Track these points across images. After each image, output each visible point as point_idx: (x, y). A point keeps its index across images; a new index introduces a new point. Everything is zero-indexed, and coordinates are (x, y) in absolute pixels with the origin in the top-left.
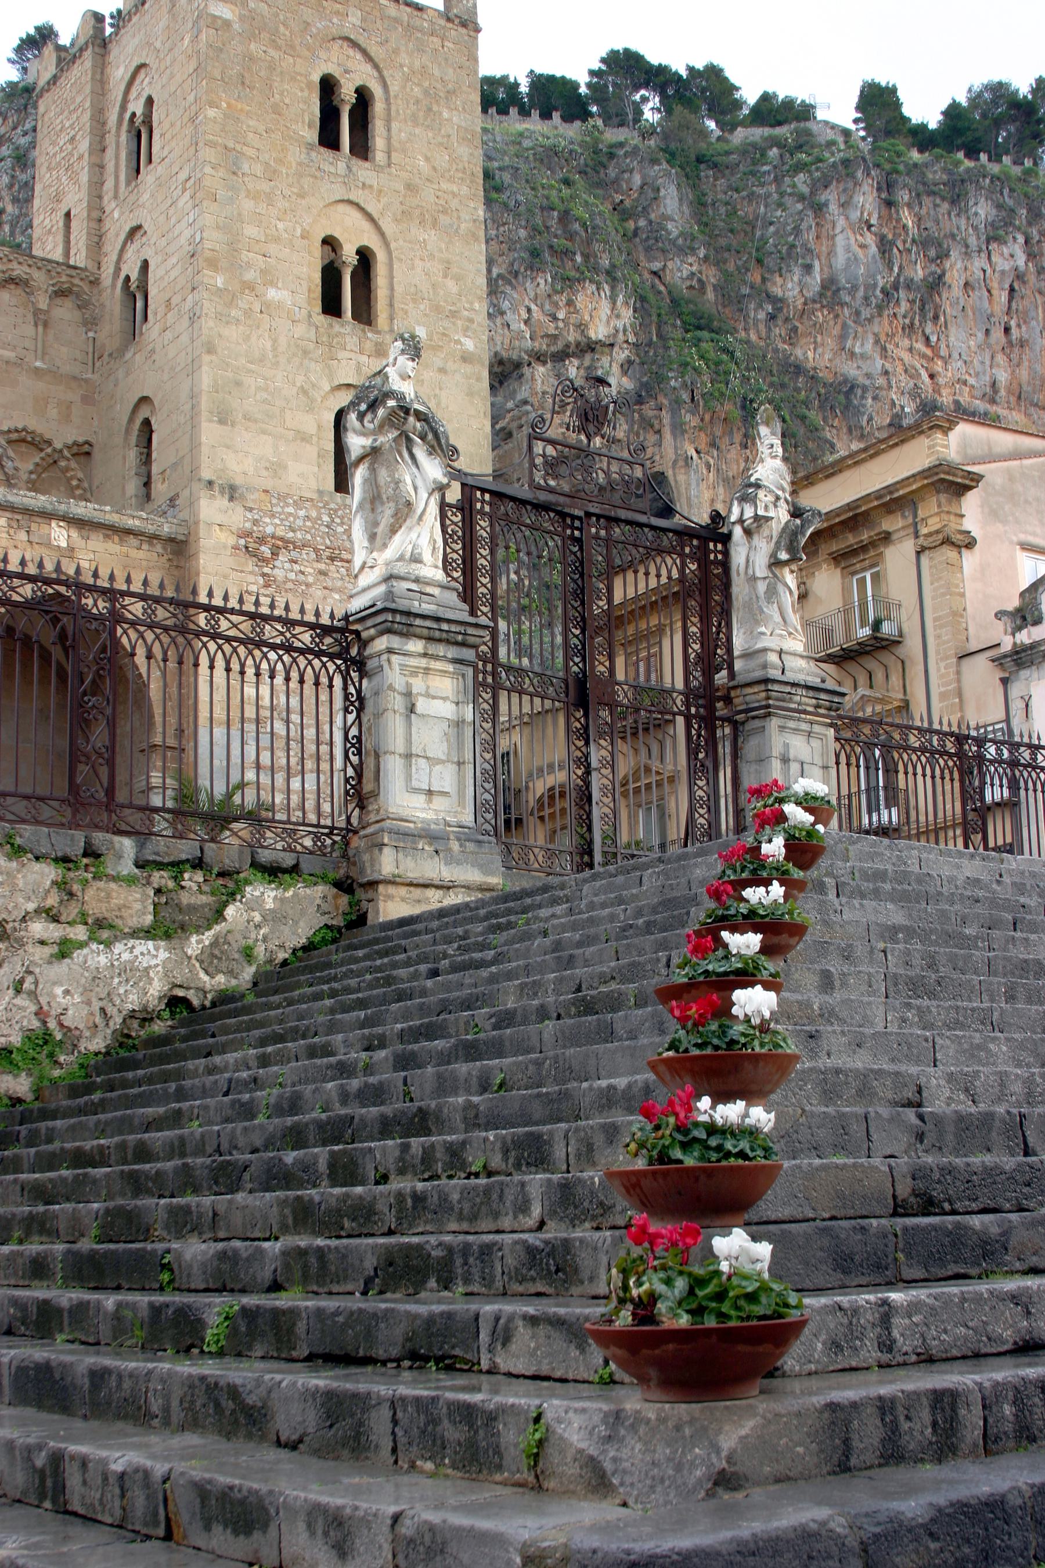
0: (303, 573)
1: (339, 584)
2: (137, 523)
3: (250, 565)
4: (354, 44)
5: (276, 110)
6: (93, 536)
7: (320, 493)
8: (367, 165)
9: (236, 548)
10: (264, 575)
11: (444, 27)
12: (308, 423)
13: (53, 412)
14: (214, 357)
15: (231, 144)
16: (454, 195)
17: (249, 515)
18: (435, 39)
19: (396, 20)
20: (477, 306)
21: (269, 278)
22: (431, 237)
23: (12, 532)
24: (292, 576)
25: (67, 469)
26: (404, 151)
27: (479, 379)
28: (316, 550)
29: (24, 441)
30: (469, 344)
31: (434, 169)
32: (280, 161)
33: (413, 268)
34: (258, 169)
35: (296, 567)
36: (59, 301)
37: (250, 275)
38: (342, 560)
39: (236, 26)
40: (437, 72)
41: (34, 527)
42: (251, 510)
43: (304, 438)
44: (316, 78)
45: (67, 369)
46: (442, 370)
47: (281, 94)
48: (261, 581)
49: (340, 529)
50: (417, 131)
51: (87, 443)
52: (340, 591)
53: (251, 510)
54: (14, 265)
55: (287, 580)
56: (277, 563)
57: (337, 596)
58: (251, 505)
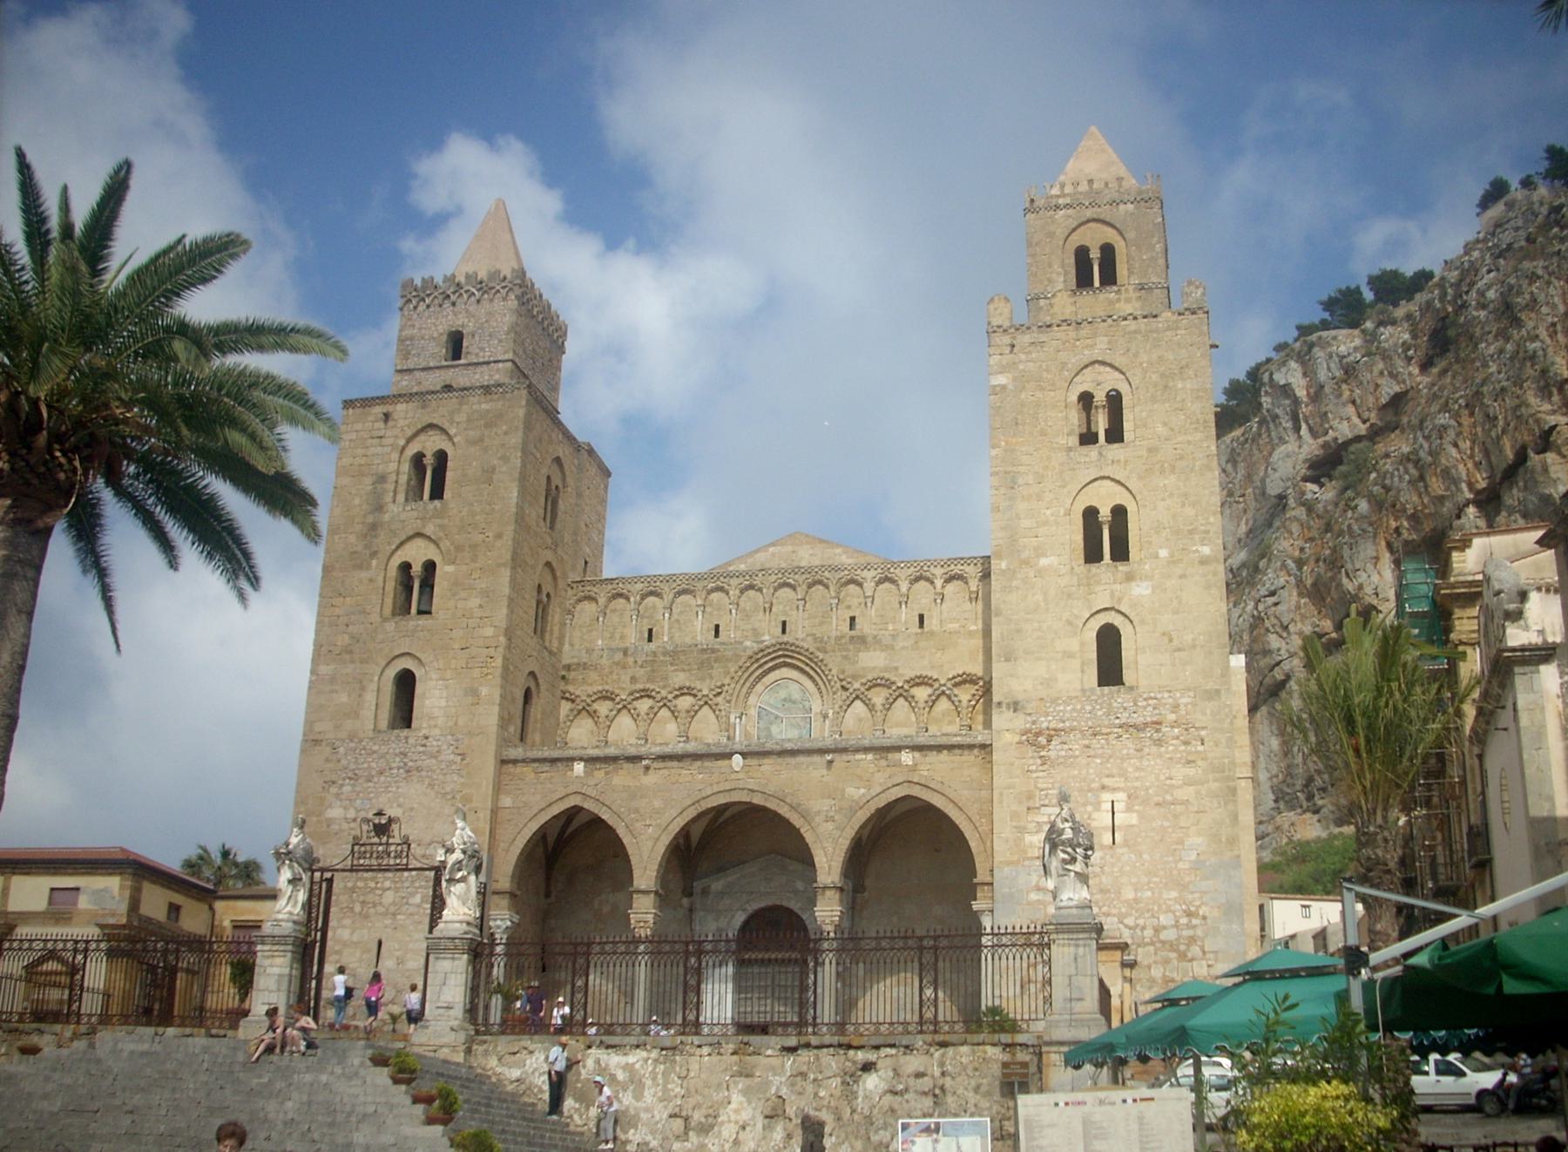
1: (1100, 751)
2: (959, 738)
3: (1030, 751)
4: (1103, 363)
5: (1043, 433)
6: (929, 753)
7: (1083, 691)
8: (1116, 446)
9: (1018, 743)
10: (1041, 757)
11: (1176, 321)
12: (1074, 644)
14: (1001, 618)
15: (1009, 469)
16: (1189, 443)
17: (1029, 719)
18: (1169, 333)
19: (1135, 332)
20: (1212, 519)
21: (1040, 552)
22: (1170, 481)
24: (1063, 753)
26: (1145, 425)
27: (1215, 574)
28: (1082, 732)
30: (1206, 550)
31: (1172, 429)
32: (1046, 468)
33: (1155, 508)
34: (1030, 479)
35: (1066, 747)
37: (1024, 555)
39: (1011, 387)
40: (1171, 357)
41: (890, 756)
42: (1030, 714)
43: (1069, 655)
44: (1074, 398)
46: (1182, 576)
47: (1046, 421)
48: (1039, 761)
49: (1100, 713)
50: (1156, 406)
52: (1101, 756)
53: (1030, 714)
55: (1059, 757)
57: (1098, 761)
58: (1029, 711)
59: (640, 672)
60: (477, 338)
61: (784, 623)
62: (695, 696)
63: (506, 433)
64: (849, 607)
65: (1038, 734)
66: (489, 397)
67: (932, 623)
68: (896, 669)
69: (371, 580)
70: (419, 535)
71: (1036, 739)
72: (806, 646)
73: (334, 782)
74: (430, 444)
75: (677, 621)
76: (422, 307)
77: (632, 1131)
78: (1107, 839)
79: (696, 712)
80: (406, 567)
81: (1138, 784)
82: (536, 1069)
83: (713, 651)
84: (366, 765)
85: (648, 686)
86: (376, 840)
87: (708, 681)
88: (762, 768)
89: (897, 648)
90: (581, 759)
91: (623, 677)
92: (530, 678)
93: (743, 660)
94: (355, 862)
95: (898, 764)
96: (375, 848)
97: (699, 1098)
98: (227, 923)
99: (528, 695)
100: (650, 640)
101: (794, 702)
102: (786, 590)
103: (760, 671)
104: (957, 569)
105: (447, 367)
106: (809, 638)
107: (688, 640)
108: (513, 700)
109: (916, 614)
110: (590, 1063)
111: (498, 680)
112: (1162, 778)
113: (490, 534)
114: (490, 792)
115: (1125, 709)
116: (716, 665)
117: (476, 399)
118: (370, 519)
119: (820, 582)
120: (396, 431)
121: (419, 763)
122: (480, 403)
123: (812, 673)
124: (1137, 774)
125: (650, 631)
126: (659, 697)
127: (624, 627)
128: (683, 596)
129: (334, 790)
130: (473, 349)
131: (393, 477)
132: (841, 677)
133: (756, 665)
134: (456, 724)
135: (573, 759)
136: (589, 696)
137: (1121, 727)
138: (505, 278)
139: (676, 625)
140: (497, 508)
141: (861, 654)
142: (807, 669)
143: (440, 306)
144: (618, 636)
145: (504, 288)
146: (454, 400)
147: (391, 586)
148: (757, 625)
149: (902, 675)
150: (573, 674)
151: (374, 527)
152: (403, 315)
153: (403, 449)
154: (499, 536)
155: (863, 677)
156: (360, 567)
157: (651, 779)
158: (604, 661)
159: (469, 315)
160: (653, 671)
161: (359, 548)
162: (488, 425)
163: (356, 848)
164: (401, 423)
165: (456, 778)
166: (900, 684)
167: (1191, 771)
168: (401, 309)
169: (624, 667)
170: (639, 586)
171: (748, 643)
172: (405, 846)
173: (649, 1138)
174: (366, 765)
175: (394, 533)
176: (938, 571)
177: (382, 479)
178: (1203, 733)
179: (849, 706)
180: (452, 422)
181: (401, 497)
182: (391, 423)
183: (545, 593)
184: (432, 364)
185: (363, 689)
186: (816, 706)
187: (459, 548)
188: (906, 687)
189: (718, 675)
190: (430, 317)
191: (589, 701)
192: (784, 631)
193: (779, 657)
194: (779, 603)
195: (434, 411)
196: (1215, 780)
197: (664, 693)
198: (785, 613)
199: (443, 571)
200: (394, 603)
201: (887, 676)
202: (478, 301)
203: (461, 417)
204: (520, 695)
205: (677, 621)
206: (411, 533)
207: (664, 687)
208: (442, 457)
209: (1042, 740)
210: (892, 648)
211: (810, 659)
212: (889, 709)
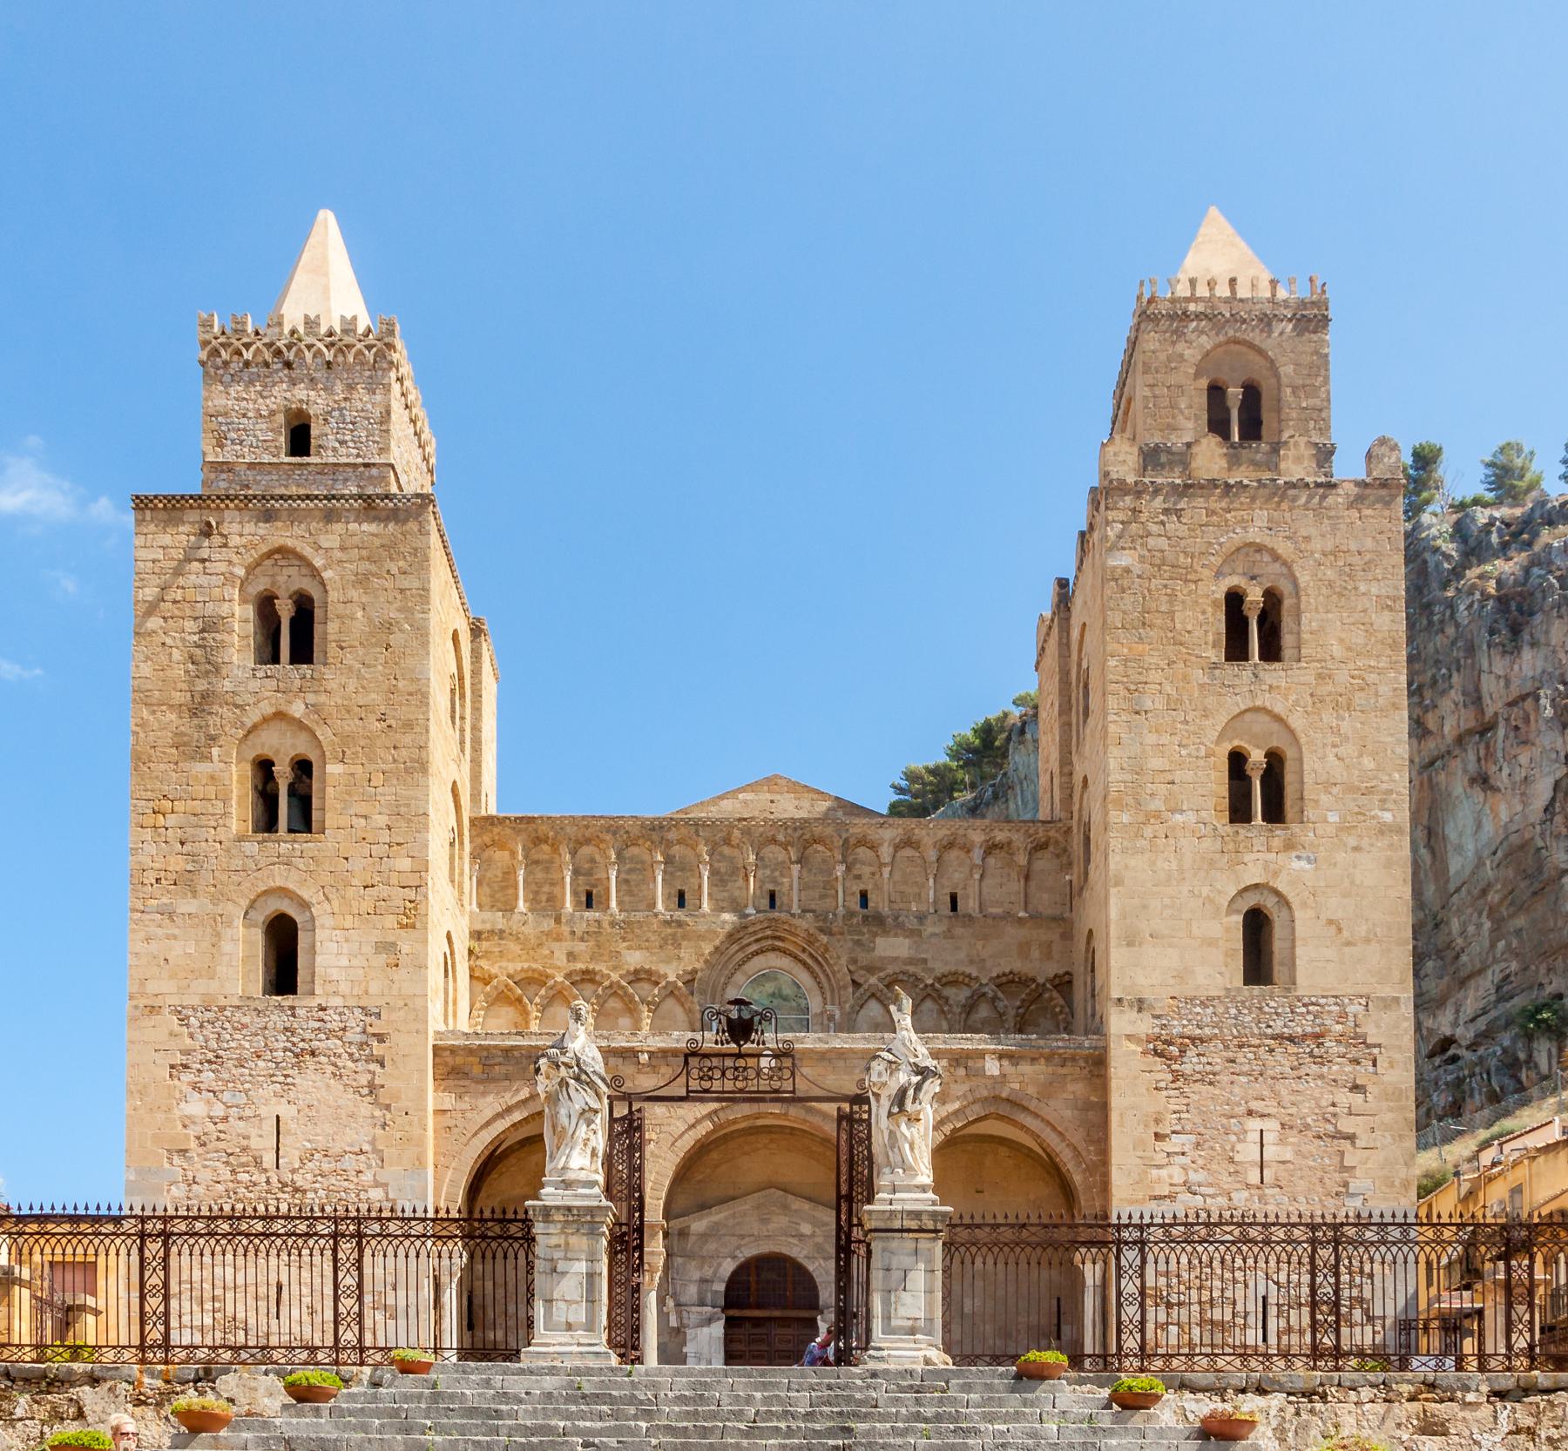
0: (1209, 1063)
2: (1060, 1044)
13: (1035, 953)
24: (1198, 1068)
25: (1051, 999)
29: (1013, 981)
35: (1204, 1060)
36: (1039, 854)
38: (1249, 1046)
45: (1049, 912)
48: (1170, 1077)
51: (1067, 973)
54: (996, 832)
56: (1185, 1059)
57: (1243, 1079)
58: (1158, 1012)
59: (581, 947)
61: (772, 896)
64: (858, 877)
65: (1169, 1043)
67: (969, 905)
68: (925, 961)
71: (1161, 1048)
73: (186, 1066)
75: (627, 881)
78: (1254, 1177)
81: (1293, 1110)
83: (680, 924)
84: (233, 1044)
85: (591, 967)
87: (675, 963)
89: (925, 934)
91: (557, 954)
95: (981, 1073)
101: (785, 999)
102: (776, 849)
103: (741, 955)
104: (1000, 836)
106: (809, 915)
109: (948, 891)
112: (1324, 1103)
115: (1277, 1014)
116: (684, 943)
121: (315, 1044)
124: (1293, 1098)
125: (589, 895)
129: (187, 1077)
132: (852, 968)
133: (735, 947)
137: (1273, 1038)
139: (624, 887)
141: (879, 940)
144: (544, 898)
148: (737, 893)
149: (932, 970)
155: (881, 969)
158: (527, 930)
165: (374, 1067)
166: (930, 982)
167: (1359, 1098)
169: (558, 939)
170: (571, 831)
174: (233, 1044)
176: (977, 837)
178: (1376, 1051)
186: (815, 1004)
188: (937, 985)
192: (772, 904)
193: (767, 938)
194: (765, 867)
196: (1391, 1110)
197: (615, 977)
198: (775, 881)
201: (911, 969)
209: (1174, 1050)
210: (919, 933)
211: (810, 943)
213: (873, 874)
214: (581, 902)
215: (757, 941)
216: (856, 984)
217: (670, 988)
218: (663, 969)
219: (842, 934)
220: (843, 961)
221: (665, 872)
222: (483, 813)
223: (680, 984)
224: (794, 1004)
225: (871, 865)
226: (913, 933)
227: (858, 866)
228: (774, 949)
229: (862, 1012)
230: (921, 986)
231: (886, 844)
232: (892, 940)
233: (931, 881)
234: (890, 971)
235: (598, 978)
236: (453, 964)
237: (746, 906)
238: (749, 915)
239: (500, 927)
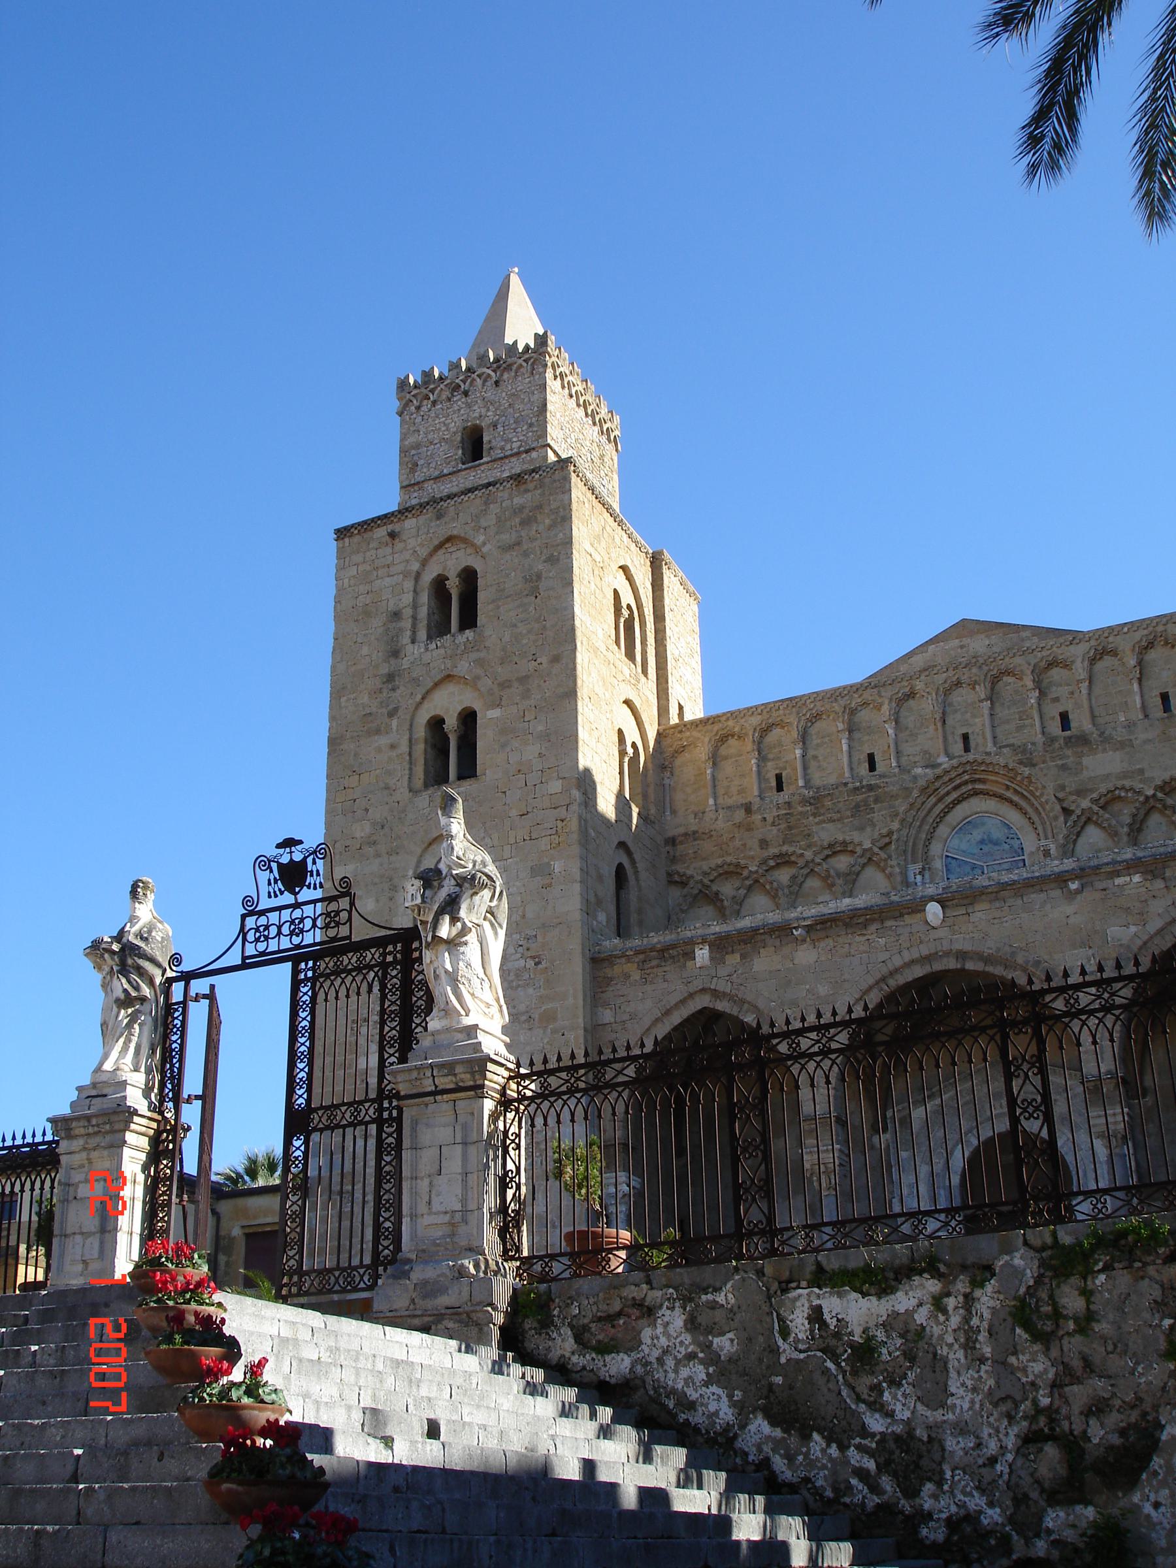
23: (1148, 884)
60: (500, 429)
61: (966, 737)
62: (853, 852)
63: (550, 528)
64: (1056, 700)
66: (523, 488)
68: (1141, 771)
69: (393, 747)
70: (449, 677)
72: (1002, 762)
74: (451, 563)
76: (427, 405)
77: (929, 1487)
79: (858, 874)
80: (437, 724)
82: (666, 1351)
83: (871, 788)
85: (785, 848)
86: (288, 899)
87: (869, 829)
88: (973, 918)
90: (704, 942)
92: (621, 852)
93: (915, 793)
94: (250, 950)
96: (286, 915)
97: (1100, 1384)
98: (237, 1232)
99: (620, 872)
100: (780, 788)
101: (996, 843)
103: (941, 806)
105: (465, 469)
106: (1005, 750)
107: (832, 780)
108: (600, 878)
109: (1156, 692)
110: (799, 1322)
111: (576, 849)
113: (544, 660)
114: (581, 1002)
116: (877, 807)
117: (506, 494)
118: (384, 669)
119: (1008, 672)
120: (407, 555)
122: (511, 498)
123: (1016, 798)
125: (779, 778)
126: (801, 862)
127: (743, 776)
128: (818, 724)
130: (496, 443)
131: (408, 612)
132: (1061, 795)
133: (933, 800)
134: (524, 916)
135: (691, 943)
136: (705, 874)
138: (527, 347)
140: (548, 625)
141: (1086, 761)
142: (1009, 794)
143: (449, 399)
144: (734, 790)
145: (526, 361)
146: (478, 501)
147: (420, 748)
150: (680, 848)
151: (390, 678)
152: (403, 422)
153: (418, 576)
154: (556, 659)
155: (1092, 791)
156: (378, 732)
157: (806, 955)
158: (720, 824)
159: (487, 403)
160: (790, 828)
161: (374, 710)
162: (525, 523)
163: (250, 922)
164: (412, 543)
166: (1150, 792)
168: (400, 414)
169: (749, 829)
170: (755, 720)
171: (919, 771)
172: (344, 903)
173: (976, 1502)
175: (416, 681)
177: (396, 615)
179: (1078, 834)
180: (477, 529)
181: (422, 634)
182: (399, 546)
183: (629, 744)
184: (445, 471)
185: (394, 888)
186: (1030, 842)
187: (505, 685)
189: (883, 821)
190: (437, 417)
191: (706, 881)
192: (967, 749)
193: (966, 783)
195: (453, 519)
197: (809, 855)
199: (488, 717)
200: (426, 772)
201: (1127, 783)
202: (497, 383)
203: (489, 520)
204: (609, 872)
205: (815, 757)
206: (439, 677)
207: (809, 846)
208: (469, 577)
211: (1012, 779)
212: (1140, 830)
213: (1072, 693)
214: (771, 788)
215: (956, 788)
216: (1067, 812)
217: (868, 855)
218: (856, 837)
219: (1044, 762)
220: (1050, 790)
221: (850, 739)
222: (674, 719)
223: (876, 850)
224: (1007, 847)
225: (1068, 685)
226: (1122, 745)
227: (1054, 688)
228: (976, 793)
229: (1081, 841)
230: (1142, 799)
231: (1079, 660)
232: (1100, 756)
233: (1136, 686)
234: (1103, 790)
235: (793, 858)
236: (636, 872)
237: (938, 756)
238: (940, 765)
239: (694, 828)
